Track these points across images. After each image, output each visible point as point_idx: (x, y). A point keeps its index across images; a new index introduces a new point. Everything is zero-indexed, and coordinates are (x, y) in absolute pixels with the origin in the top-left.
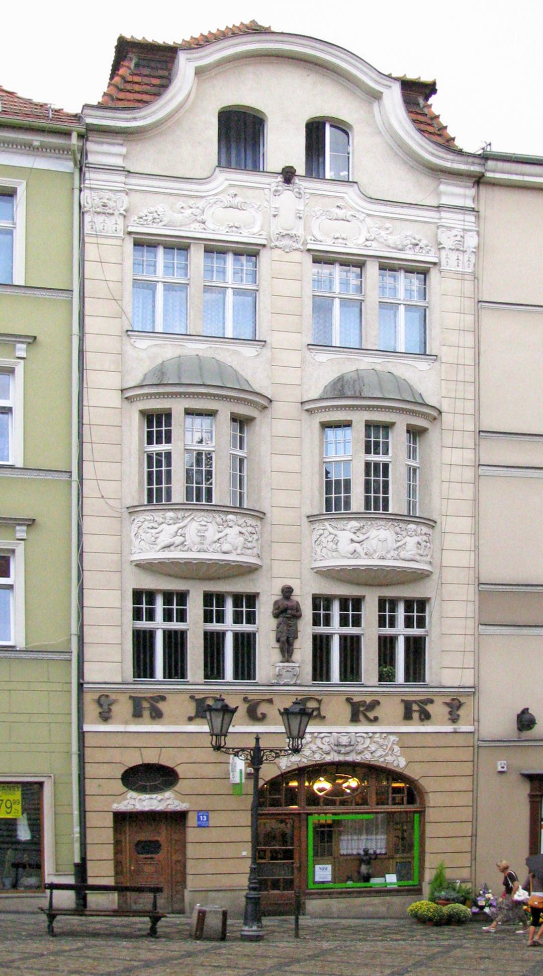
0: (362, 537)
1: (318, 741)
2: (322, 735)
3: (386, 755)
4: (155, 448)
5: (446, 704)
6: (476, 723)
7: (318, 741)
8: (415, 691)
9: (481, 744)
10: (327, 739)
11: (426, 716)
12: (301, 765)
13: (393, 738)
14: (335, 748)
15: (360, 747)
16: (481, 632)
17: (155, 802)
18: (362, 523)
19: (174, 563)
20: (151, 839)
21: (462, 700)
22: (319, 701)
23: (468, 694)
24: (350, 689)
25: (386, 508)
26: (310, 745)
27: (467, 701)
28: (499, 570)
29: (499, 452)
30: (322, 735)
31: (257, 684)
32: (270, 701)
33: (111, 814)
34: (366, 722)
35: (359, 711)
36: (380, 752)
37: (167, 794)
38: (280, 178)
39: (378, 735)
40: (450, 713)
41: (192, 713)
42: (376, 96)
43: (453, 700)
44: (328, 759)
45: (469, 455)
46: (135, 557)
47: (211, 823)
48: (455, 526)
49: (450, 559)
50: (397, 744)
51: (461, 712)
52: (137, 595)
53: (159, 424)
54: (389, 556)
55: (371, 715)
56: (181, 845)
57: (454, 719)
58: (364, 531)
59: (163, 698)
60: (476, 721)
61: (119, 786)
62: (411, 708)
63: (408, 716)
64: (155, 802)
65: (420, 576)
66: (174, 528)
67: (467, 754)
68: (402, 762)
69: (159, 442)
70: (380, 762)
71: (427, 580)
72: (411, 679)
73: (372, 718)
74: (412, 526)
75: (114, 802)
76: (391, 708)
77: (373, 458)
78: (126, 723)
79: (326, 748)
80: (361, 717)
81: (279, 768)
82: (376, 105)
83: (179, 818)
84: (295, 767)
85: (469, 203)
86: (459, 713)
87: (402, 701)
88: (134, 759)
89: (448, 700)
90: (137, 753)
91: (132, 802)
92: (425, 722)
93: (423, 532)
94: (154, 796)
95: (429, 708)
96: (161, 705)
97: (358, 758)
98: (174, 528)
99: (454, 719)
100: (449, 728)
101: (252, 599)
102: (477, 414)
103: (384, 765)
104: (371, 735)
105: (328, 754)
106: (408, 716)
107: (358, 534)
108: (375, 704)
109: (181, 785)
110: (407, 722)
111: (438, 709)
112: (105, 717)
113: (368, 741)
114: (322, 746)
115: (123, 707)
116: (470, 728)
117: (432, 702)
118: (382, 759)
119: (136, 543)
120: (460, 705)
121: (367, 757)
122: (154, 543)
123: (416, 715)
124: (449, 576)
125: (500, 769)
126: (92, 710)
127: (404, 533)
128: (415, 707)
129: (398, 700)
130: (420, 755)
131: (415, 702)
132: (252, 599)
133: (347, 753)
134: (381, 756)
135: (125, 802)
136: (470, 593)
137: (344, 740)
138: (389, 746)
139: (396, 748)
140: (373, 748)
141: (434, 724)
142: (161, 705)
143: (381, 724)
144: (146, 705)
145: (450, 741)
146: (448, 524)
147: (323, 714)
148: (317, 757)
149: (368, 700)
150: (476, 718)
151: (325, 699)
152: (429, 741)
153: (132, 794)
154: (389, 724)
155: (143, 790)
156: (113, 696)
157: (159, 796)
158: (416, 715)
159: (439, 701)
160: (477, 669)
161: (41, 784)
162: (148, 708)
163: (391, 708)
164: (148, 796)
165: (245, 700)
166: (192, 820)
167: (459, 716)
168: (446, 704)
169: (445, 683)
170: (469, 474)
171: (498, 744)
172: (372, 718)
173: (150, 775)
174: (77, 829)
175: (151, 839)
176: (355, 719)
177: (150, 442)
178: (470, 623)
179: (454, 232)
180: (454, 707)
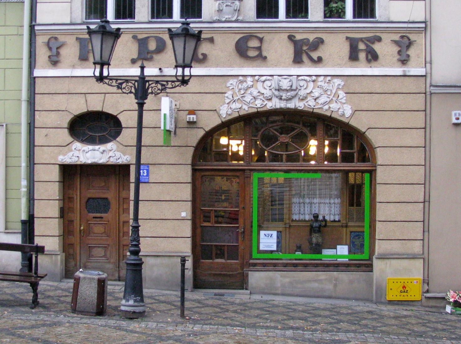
1: (259, 85)
2: (263, 78)
5: (396, 42)
6: (428, 65)
7: (259, 85)
10: (268, 83)
11: (373, 57)
12: (242, 113)
14: (277, 93)
15: (302, 93)
17: (97, 154)
22: (261, 40)
24: (296, 24)
26: (252, 90)
30: (263, 78)
33: (57, 166)
34: (310, 63)
35: (304, 51)
39: (322, 78)
40: (399, 52)
44: (270, 105)
50: (342, 89)
51: (412, 52)
57: (404, 61)
60: (428, 62)
62: (357, 47)
63: (353, 57)
64: (97, 154)
73: (316, 59)
75: (59, 154)
79: (268, 93)
80: (305, 58)
81: (220, 116)
84: (236, 115)
86: (409, 53)
91: (76, 153)
92: (374, 63)
94: (97, 147)
95: (377, 47)
99: (404, 61)
100: (398, 71)
104: (314, 78)
105: (270, 100)
106: (353, 57)
113: (311, 85)
114: (263, 91)
116: (421, 71)
120: (410, 44)
123: (362, 56)
128: (362, 46)
133: (289, 100)
135: (70, 154)
137: (285, 84)
138: (334, 91)
139: (342, 94)
140: (316, 94)
141: (383, 66)
143: (324, 66)
147: (264, 54)
148: (258, 103)
149: (312, 37)
150: (428, 59)
153: (77, 145)
154: (334, 66)
155: (91, 141)
157: (102, 147)
158: (362, 56)
164: (91, 147)
167: (408, 56)
172: (316, 59)
174: (24, 183)
176: (297, 60)
180: (404, 45)
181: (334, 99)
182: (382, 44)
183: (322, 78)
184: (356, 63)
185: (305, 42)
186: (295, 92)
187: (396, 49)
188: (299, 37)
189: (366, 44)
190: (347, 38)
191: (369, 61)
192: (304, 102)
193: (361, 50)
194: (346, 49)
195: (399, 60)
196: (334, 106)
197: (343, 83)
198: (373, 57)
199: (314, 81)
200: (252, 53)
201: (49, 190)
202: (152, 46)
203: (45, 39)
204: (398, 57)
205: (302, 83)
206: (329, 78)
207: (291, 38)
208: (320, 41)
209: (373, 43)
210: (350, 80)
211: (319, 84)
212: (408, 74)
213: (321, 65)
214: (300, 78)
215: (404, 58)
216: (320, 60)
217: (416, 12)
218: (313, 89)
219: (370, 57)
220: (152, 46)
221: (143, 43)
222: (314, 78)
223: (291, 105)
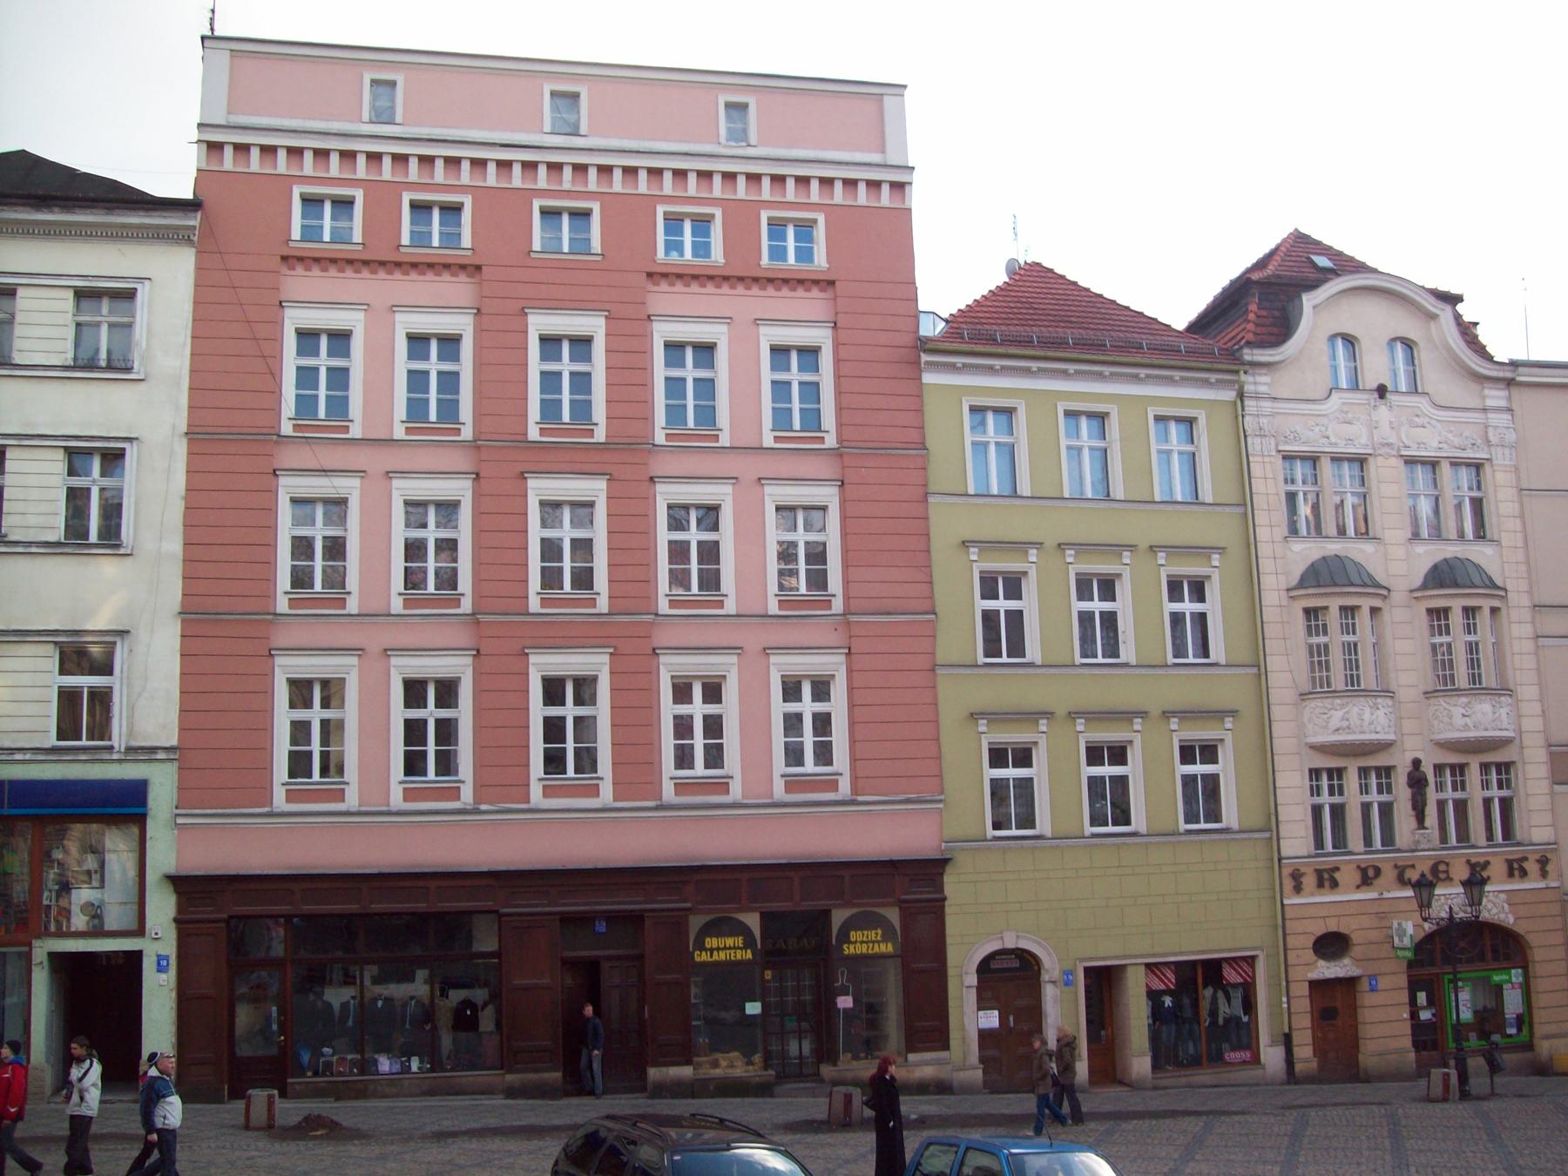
4: (1315, 640)
8: (1514, 851)
11: (1524, 873)
13: (1503, 896)
19: (1343, 744)
20: (1334, 1004)
21: (1549, 856)
31: (1399, 851)
32: (1413, 866)
36: (1495, 911)
37: (1346, 961)
38: (1376, 395)
41: (1359, 882)
42: (1433, 317)
46: (1312, 740)
47: (1381, 986)
51: (1549, 868)
52: (1315, 773)
53: (1439, 619)
56: (1353, 1008)
59: (1337, 869)
61: (1309, 955)
66: (1340, 713)
68: (1511, 920)
69: (1318, 634)
78: (1312, 895)
82: (1432, 325)
83: (1350, 983)
88: (1319, 929)
90: (1321, 921)
95: (1526, 865)
96: (1337, 875)
98: (1340, 713)
100: (1542, 885)
101: (1386, 772)
106: (1511, 874)
109: (1356, 951)
111: (1532, 867)
112: (1298, 889)
115: (1309, 881)
119: (1310, 726)
122: (1326, 727)
126: (1288, 884)
132: (1386, 772)
142: (1337, 875)
144: (1326, 876)
151: (1452, 861)
153: (1321, 963)
156: (1303, 870)
161: (1253, 958)
162: (1327, 879)
165: (1468, 862)
166: (1364, 985)
173: (1331, 944)
175: (1334, 1004)
177: (1310, 634)
180: (1543, 862)
185: (1478, 864)
188: (1473, 860)
194: (1504, 868)
198: (1524, 873)
200: (1442, 876)
201: (1303, 1004)
202: (1371, 873)
203: (1290, 870)
207: (1468, 862)
208: (1487, 863)
220: (1371, 873)
221: (1364, 871)
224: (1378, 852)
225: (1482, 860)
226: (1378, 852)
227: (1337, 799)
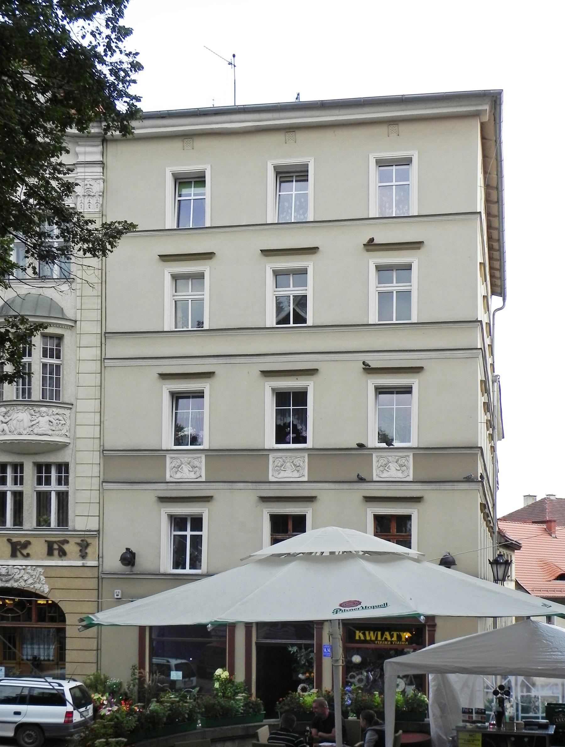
0: (8, 419)
3: (35, 583)
5: (78, 544)
6: (101, 559)
9: (104, 576)
11: (63, 554)
13: (40, 569)
15: (17, 577)
16: (105, 488)
18: (8, 408)
21: (89, 541)
23: (93, 536)
25: (29, 396)
27: (94, 542)
28: (117, 440)
29: (117, 348)
34: (22, 557)
40: (81, 551)
43: (82, 541)
45: (95, 353)
48: (87, 407)
49: (82, 432)
50: (43, 575)
51: (89, 550)
54: (25, 432)
55: (25, 552)
57: (84, 556)
58: (9, 414)
62: (52, 546)
63: (50, 553)
65: (61, 447)
67: (93, 584)
68: (46, 589)
70: (31, 588)
71: (66, 448)
72: (61, 525)
74: (43, 409)
76: (38, 547)
77: (54, 361)
80: (18, 554)
85: (98, 158)
87: (46, 541)
89: (78, 540)
92: (63, 558)
93: (55, 413)
95: (66, 547)
97: (15, 585)
99: (84, 556)
100: (80, 563)
102: (103, 320)
103: (33, 591)
104: (24, 567)
106: (50, 553)
107: (6, 417)
108: (27, 544)
110: (50, 557)
111: (71, 548)
116: (95, 563)
117: (67, 542)
118: (32, 586)
120: (88, 545)
121: (21, 584)
123: (56, 553)
124: (81, 445)
125: (116, 597)
127: (38, 415)
128: (56, 546)
129: (43, 540)
130: (59, 583)
131: (55, 542)
133: (7, 581)
134: (32, 584)
136: (96, 457)
139: (42, 577)
140: (26, 578)
141: (70, 560)
145: (78, 573)
146: (80, 406)
150: (100, 555)
152: (66, 573)
158: (56, 553)
159: (72, 541)
160: (101, 516)
163: (38, 547)
167: (86, 553)
168: (78, 544)
169: (77, 528)
170: (96, 366)
171: (115, 576)
176: (14, 555)
178: (96, 481)
179: (86, 182)
180: (84, 546)
181: (38, 581)
182: (70, 544)
183: (30, 567)
184: (53, 558)
185: (18, 543)
186: (11, 577)
187: (79, 548)
188: (14, 540)
189: (58, 545)
190: (46, 541)
191: (60, 556)
192: (18, 583)
193: (55, 549)
194: (44, 548)
195: (80, 556)
196: (37, 586)
197: (43, 571)
199: (24, 569)
204: (80, 554)
205: (16, 570)
206: (34, 567)
207: (9, 540)
209: (63, 544)
210: (47, 569)
211: (28, 571)
212: (86, 565)
213: (29, 558)
214: (15, 567)
215: (84, 555)
216: (28, 555)
217: (93, 524)
218: (24, 574)
219: (61, 554)
222: (24, 567)
223: (8, 585)
224: (53, 530)
225: (23, 540)
226: (53, 530)
227: (62, 488)
